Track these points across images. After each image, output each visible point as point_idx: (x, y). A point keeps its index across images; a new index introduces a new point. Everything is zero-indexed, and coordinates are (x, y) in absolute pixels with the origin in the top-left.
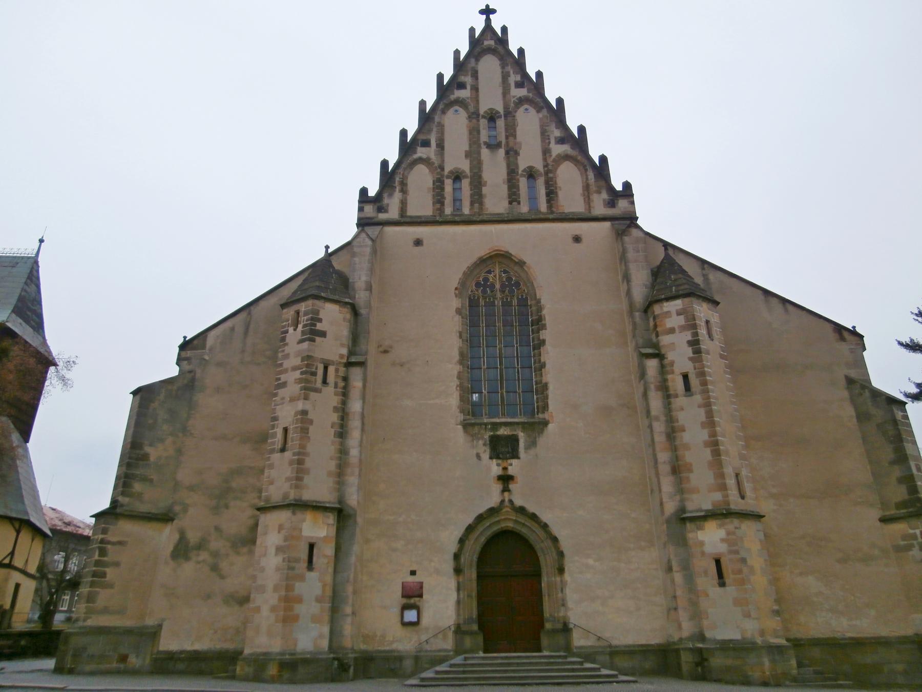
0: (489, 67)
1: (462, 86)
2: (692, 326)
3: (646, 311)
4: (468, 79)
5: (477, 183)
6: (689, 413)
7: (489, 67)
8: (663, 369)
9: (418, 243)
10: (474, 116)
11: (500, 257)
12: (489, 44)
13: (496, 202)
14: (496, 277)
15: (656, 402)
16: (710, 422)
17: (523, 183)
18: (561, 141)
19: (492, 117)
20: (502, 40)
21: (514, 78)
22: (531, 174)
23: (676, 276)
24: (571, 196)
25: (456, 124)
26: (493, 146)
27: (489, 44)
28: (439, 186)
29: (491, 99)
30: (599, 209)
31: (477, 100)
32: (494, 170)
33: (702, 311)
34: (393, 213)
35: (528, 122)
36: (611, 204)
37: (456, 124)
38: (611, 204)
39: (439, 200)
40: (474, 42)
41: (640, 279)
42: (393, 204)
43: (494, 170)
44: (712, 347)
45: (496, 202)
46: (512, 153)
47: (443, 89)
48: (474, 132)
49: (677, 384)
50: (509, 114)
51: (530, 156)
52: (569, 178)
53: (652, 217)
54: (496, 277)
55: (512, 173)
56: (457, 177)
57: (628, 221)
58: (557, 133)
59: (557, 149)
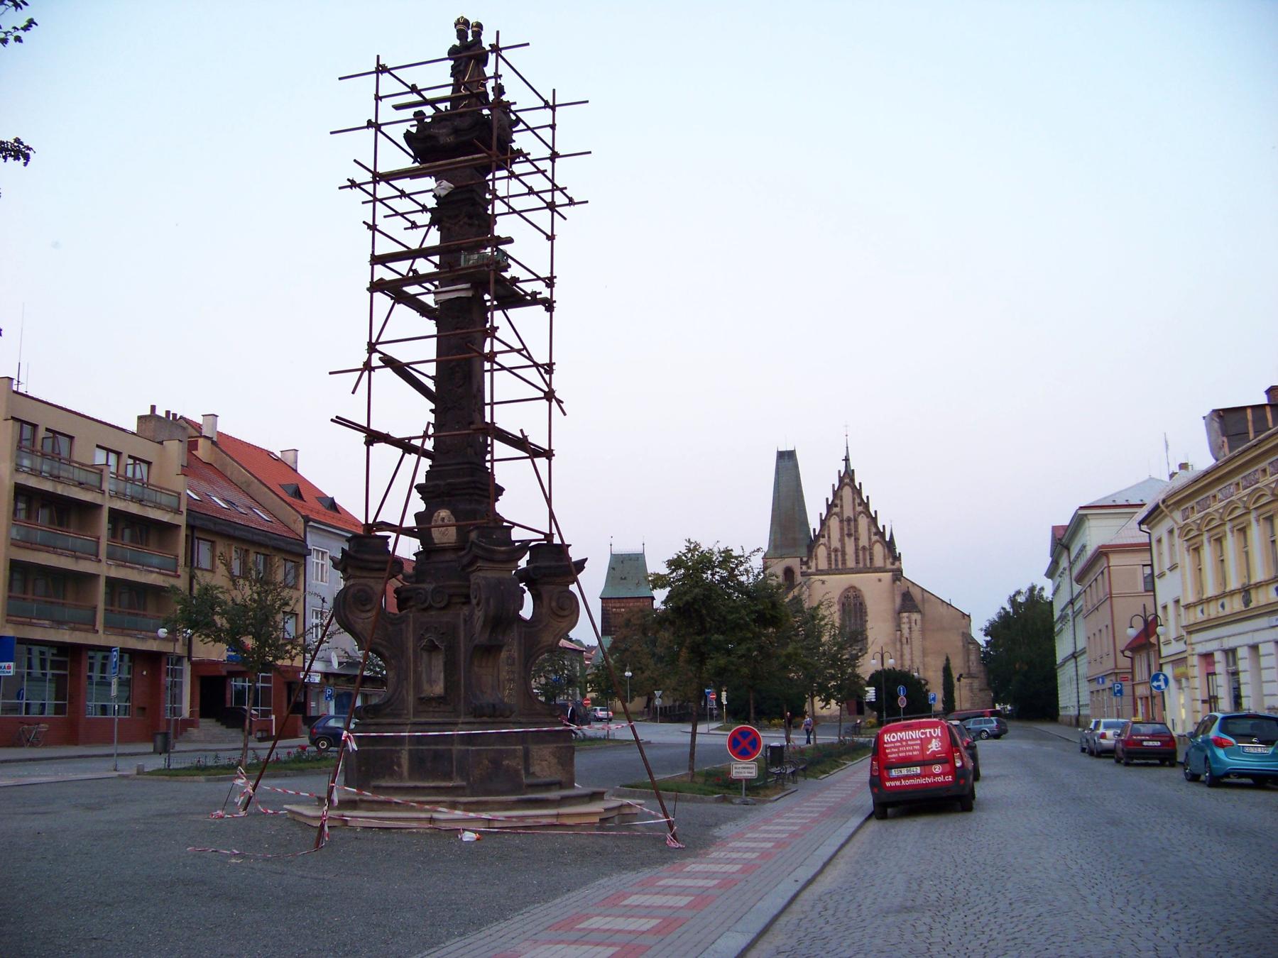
0: (847, 492)
1: (836, 506)
2: (910, 622)
3: (899, 613)
4: (838, 502)
5: (844, 554)
6: (907, 649)
7: (847, 492)
8: (902, 635)
9: (823, 582)
10: (841, 521)
11: (853, 587)
12: (847, 478)
13: (851, 563)
14: (851, 594)
15: (898, 646)
16: (912, 653)
17: (861, 553)
18: (875, 534)
19: (849, 520)
20: (852, 480)
21: (858, 501)
22: (864, 548)
23: (910, 600)
24: (879, 562)
25: (834, 523)
26: (849, 535)
27: (847, 478)
28: (829, 555)
29: (848, 512)
30: (889, 566)
31: (842, 512)
32: (850, 549)
33: (916, 616)
34: (813, 570)
35: (863, 522)
36: (893, 564)
37: (834, 523)
38: (893, 564)
39: (830, 564)
40: (841, 480)
41: (898, 601)
42: (813, 564)
43: (850, 549)
44: (916, 628)
45: (851, 563)
46: (857, 539)
47: (829, 507)
48: (842, 529)
49: (904, 640)
50: (856, 520)
51: (864, 541)
52: (878, 550)
53: (910, 570)
54: (851, 594)
55: (857, 550)
56: (836, 550)
57: (898, 575)
58: (874, 530)
59: (874, 538)
